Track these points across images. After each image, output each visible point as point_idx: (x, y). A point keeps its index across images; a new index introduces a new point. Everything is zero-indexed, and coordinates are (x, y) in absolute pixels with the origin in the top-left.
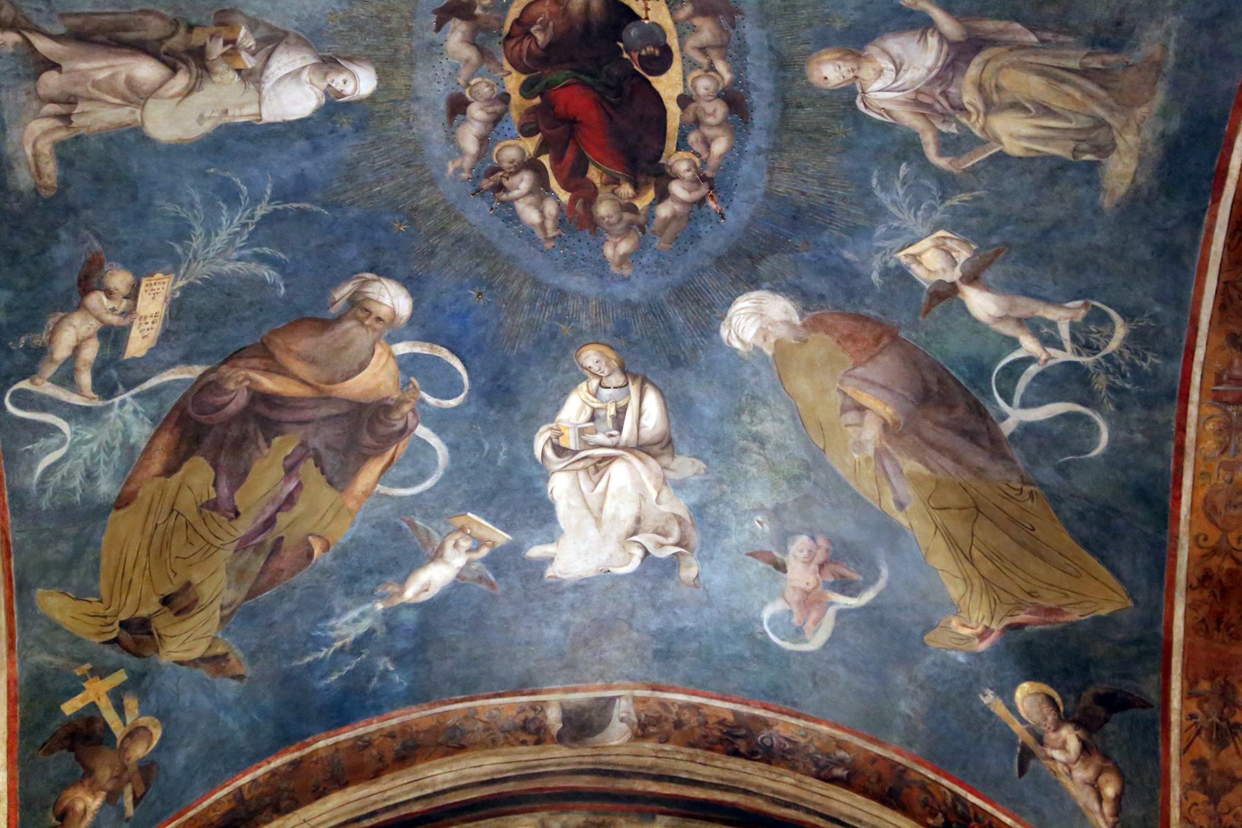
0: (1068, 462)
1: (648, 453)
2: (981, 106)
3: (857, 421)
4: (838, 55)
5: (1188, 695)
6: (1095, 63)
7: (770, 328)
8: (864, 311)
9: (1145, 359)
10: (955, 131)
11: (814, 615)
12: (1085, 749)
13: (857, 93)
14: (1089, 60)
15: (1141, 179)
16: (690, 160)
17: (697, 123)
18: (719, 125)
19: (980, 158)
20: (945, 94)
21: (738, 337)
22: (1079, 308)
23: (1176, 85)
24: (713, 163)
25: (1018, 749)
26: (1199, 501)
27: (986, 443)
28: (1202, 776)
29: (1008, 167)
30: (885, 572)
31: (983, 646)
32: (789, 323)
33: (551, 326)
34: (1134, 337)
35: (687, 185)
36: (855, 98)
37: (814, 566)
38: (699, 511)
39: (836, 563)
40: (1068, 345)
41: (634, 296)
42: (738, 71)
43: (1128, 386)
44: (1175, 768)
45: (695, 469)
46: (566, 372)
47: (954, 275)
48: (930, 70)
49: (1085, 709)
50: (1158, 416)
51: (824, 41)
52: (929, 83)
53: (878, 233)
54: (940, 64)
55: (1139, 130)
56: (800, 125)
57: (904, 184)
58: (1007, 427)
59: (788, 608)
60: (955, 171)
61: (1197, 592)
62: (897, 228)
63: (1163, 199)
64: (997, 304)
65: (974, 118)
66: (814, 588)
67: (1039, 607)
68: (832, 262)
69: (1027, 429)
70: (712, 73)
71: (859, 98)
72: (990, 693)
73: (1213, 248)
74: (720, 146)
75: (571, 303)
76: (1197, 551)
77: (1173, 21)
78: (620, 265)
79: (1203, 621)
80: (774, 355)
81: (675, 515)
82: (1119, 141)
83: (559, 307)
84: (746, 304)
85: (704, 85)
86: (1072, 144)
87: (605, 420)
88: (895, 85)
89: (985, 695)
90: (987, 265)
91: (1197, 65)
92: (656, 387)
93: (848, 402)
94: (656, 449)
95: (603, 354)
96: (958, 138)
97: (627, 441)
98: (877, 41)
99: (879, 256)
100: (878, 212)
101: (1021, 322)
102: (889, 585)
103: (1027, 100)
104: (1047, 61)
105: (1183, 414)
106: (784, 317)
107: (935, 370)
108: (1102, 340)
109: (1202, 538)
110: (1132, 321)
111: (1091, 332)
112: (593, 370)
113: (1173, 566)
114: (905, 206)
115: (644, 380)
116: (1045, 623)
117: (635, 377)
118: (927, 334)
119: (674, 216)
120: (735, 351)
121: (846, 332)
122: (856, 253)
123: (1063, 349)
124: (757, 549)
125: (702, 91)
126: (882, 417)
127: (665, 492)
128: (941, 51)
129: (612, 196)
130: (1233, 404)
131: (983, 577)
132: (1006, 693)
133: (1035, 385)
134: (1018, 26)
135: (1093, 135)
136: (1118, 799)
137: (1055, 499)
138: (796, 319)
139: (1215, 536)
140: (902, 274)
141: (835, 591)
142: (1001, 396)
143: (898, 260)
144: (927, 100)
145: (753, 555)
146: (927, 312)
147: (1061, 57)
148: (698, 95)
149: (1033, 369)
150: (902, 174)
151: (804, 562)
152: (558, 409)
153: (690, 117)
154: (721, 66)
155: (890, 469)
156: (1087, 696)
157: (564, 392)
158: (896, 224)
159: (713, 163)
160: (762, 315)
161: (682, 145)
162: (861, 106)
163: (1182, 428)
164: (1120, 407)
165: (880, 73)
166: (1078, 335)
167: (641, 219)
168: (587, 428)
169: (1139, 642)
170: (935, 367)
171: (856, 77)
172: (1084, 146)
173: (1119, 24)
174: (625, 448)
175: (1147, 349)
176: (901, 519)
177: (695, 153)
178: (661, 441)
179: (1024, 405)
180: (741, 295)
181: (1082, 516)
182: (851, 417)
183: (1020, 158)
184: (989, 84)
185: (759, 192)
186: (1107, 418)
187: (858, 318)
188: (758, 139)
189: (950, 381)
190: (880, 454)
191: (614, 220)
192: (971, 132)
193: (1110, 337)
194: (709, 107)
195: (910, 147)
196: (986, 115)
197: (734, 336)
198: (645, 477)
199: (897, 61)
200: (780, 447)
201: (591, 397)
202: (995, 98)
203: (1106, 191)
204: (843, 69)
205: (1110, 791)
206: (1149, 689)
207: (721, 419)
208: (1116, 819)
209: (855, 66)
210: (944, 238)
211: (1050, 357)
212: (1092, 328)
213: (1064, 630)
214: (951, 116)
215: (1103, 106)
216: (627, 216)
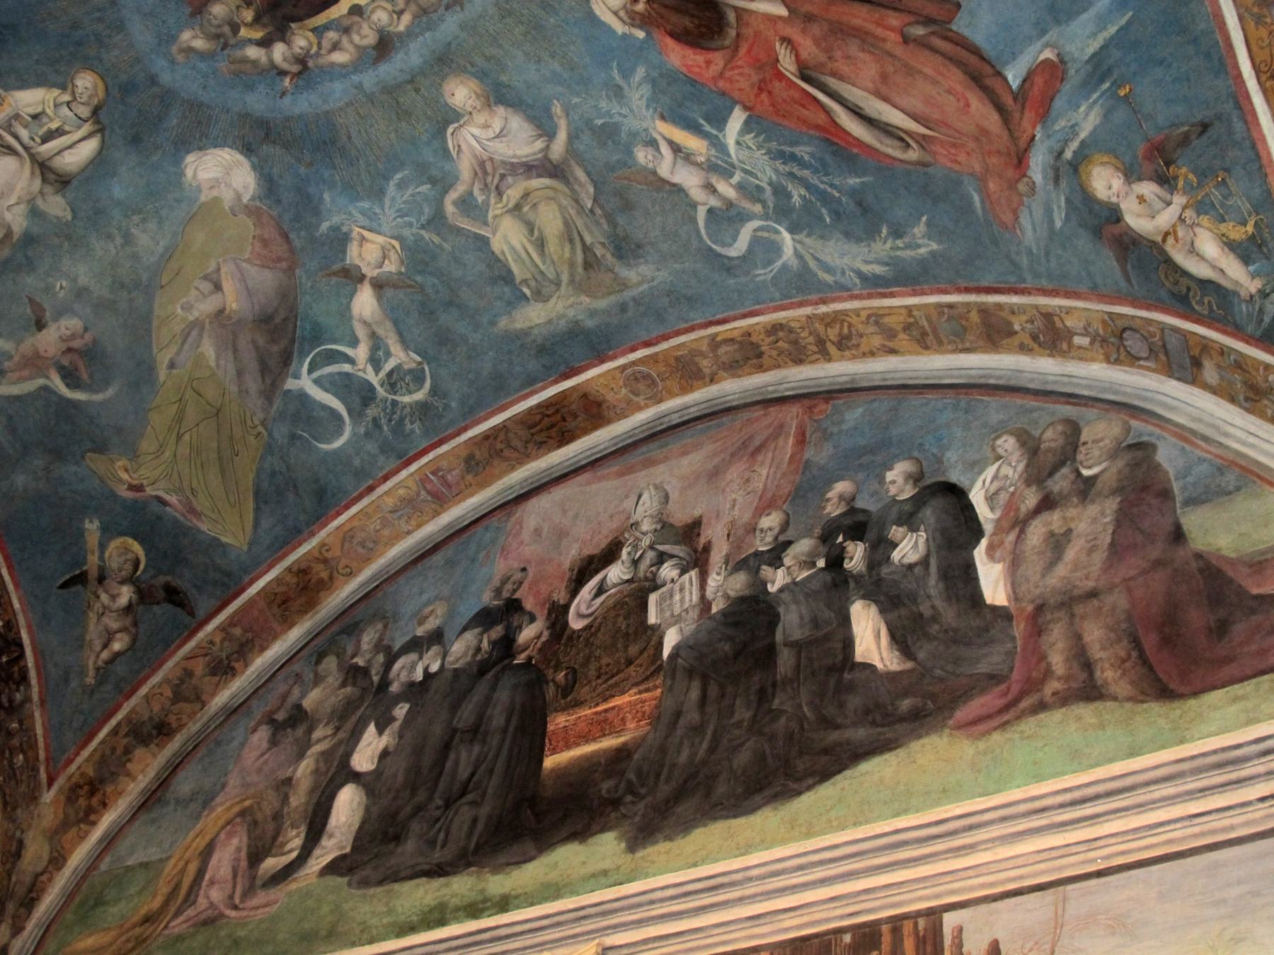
0: (301, 436)
1: (42, 173)
2: (511, 205)
3: (206, 292)
4: (479, 92)
5: (222, 628)
6: (599, 252)
7: (223, 185)
8: (292, 236)
9: (412, 423)
10: (480, 200)
11: (26, 373)
12: (129, 609)
13: (458, 121)
14: (598, 246)
15: (536, 331)
16: (311, 44)
17: (346, 31)
18: (357, 47)
19: (473, 229)
20: (503, 176)
21: (196, 169)
22: (414, 361)
23: (623, 308)
24: (321, 61)
25: (77, 572)
26: (346, 528)
27: (268, 381)
28: (182, 681)
29: (480, 250)
30: (110, 392)
31: (124, 493)
32: (239, 197)
33: (87, 35)
34: (423, 407)
35: (288, 54)
36: (453, 123)
37: (64, 347)
38: (29, 240)
39: (82, 357)
40: (382, 374)
41: (166, 78)
42: (410, 34)
43: (385, 428)
44: (170, 664)
45: (61, 214)
46: (57, 71)
47: (370, 272)
48: (515, 156)
49: (152, 586)
50: (382, 459)
51: (481, 76)
52: (503, 162)
53: (360, 204)
54: (524, 160)
55: (571, 306)
56: (401, 100)
57: (413, 195)
58: (291, 384)
59: (13, 353)
60: (450, 220)
61: (290, 575)
62: (375, 213)
63: (532, 352)
64: (373, 313)
65: (499, 206)
66: (47, 358)
67: (191, 502)
68: (312, 190)
69: (303, 396)
70: (395, 16)
71: (456, 125)
72: (97, 523)
73: (523, 403)
74: (339, 57)
75: (119, 37)
76: (316, 554)
77: (663, 275)
78: (182, 50)
79: (276, 594)
80: (203, 204)
81: (9, 227)
82: (553, 301)
83: (108, 31)
84: (228, 157)
85: (381, 17)
86: (529, 276)
87: (41, 126)
88: (485, 142)
89: (91, 522)
90: (395, 286)
91: (642, 309)
92: (103, 141)
93: (215, 276)
94: (52, 177)
95: (95, 87)
96: (476, 206)
97: (39, 153)
98: (510, 110)
99: (344, 217)
100: (379, 194)
101: (373, 335)
102: (102, 404)
103: (539, 229)
104: (579, 223)
105: (397, 471)
106: (241, 190)
107: (291, 311)
108: (404, 390)
109: (327, 548)
110: (433, 396)
111: (404, 380)
112: (76, 90)
113: (295, 548)
114: (397, 207)
115: (101, 130)
116: (183, 515)
117: (98, 122)
118: (312, 287)
119: (255, 63)
120: (182, 174)
121: (266, 236)
122: (333, 201)
123: (377, 375)
124: (38, 300)
125: (375, 17)
126: (225, 305)
127: (22, 206)
128: (535, 154)
129: (234, 8)
130: (428, 492)
131: (175, 455)
132: (109, 531)
133: (337, 377)
134: (592, 190)
135: (544, 283)
136: (118, 655)
137: (269, 448)
138: (245, 200)
139: (336, 552)
140: (340, 240)
141: (59, 373)
142: (310, 363)
143: (351, 231)
144: (489, 167)
145: (31, 300)
146: (329, 275)
147: (588, 228)
148: (369, 17)
149: (347, 368)
150: (419, 189)
151: (60, 337)
152: (24, 85)
153: (346, 22)
154: (406, 18)
155: (190, 340)
156: (162, 579)
157: (41, 82)
158: (378, 210)
159: (321, 61)
160: (228, 173)
161: (319, 31)
162: (450, 130)
163: (386, 478)
164: (367, 434)
165: (486, 126)
166: (395, 376)
167: (232, 41)
168: (23, 118)
169: (229, 575)
170: (293, 310)
171: (471, 113)
172: (533, 283)
173: (639, 246)
174: (33, 157)
175: (420, 419)
176: (162, 374)
177: (319, 44)
178: (61, 176)
179: (317, 382)
180: (232, 148)
181: (273, 474)
182: (207, 287)
183: (493, 253)
184: (533, 198)
185: (326, 108)
186: (354, 434)
187: (286, 236)
188: (369, 79)
189: (291, 326)
190: (197, 324)
191: (215, 22)
192: (487, 211)
193: (410, 393)
194: (366, 30)
195: (443, 183)
196: (507, 212)
197: (193, 167)
198: (19, 186)
199: (504, 132)
200: (135, 257)
201: (52, 104)
202: (526, 209)
203: (511, 317)
204: (470, 102)
205: (117, 646)
206: (202, 607)
207: (119, 203)
208: (104, 665)
209: (479, 107)
210: (394, 247)
211: (364, 371)
212: (408, 378)
213: (190, 528)
214: (489, 191)
215: (572, 275)
216: (226, 29)
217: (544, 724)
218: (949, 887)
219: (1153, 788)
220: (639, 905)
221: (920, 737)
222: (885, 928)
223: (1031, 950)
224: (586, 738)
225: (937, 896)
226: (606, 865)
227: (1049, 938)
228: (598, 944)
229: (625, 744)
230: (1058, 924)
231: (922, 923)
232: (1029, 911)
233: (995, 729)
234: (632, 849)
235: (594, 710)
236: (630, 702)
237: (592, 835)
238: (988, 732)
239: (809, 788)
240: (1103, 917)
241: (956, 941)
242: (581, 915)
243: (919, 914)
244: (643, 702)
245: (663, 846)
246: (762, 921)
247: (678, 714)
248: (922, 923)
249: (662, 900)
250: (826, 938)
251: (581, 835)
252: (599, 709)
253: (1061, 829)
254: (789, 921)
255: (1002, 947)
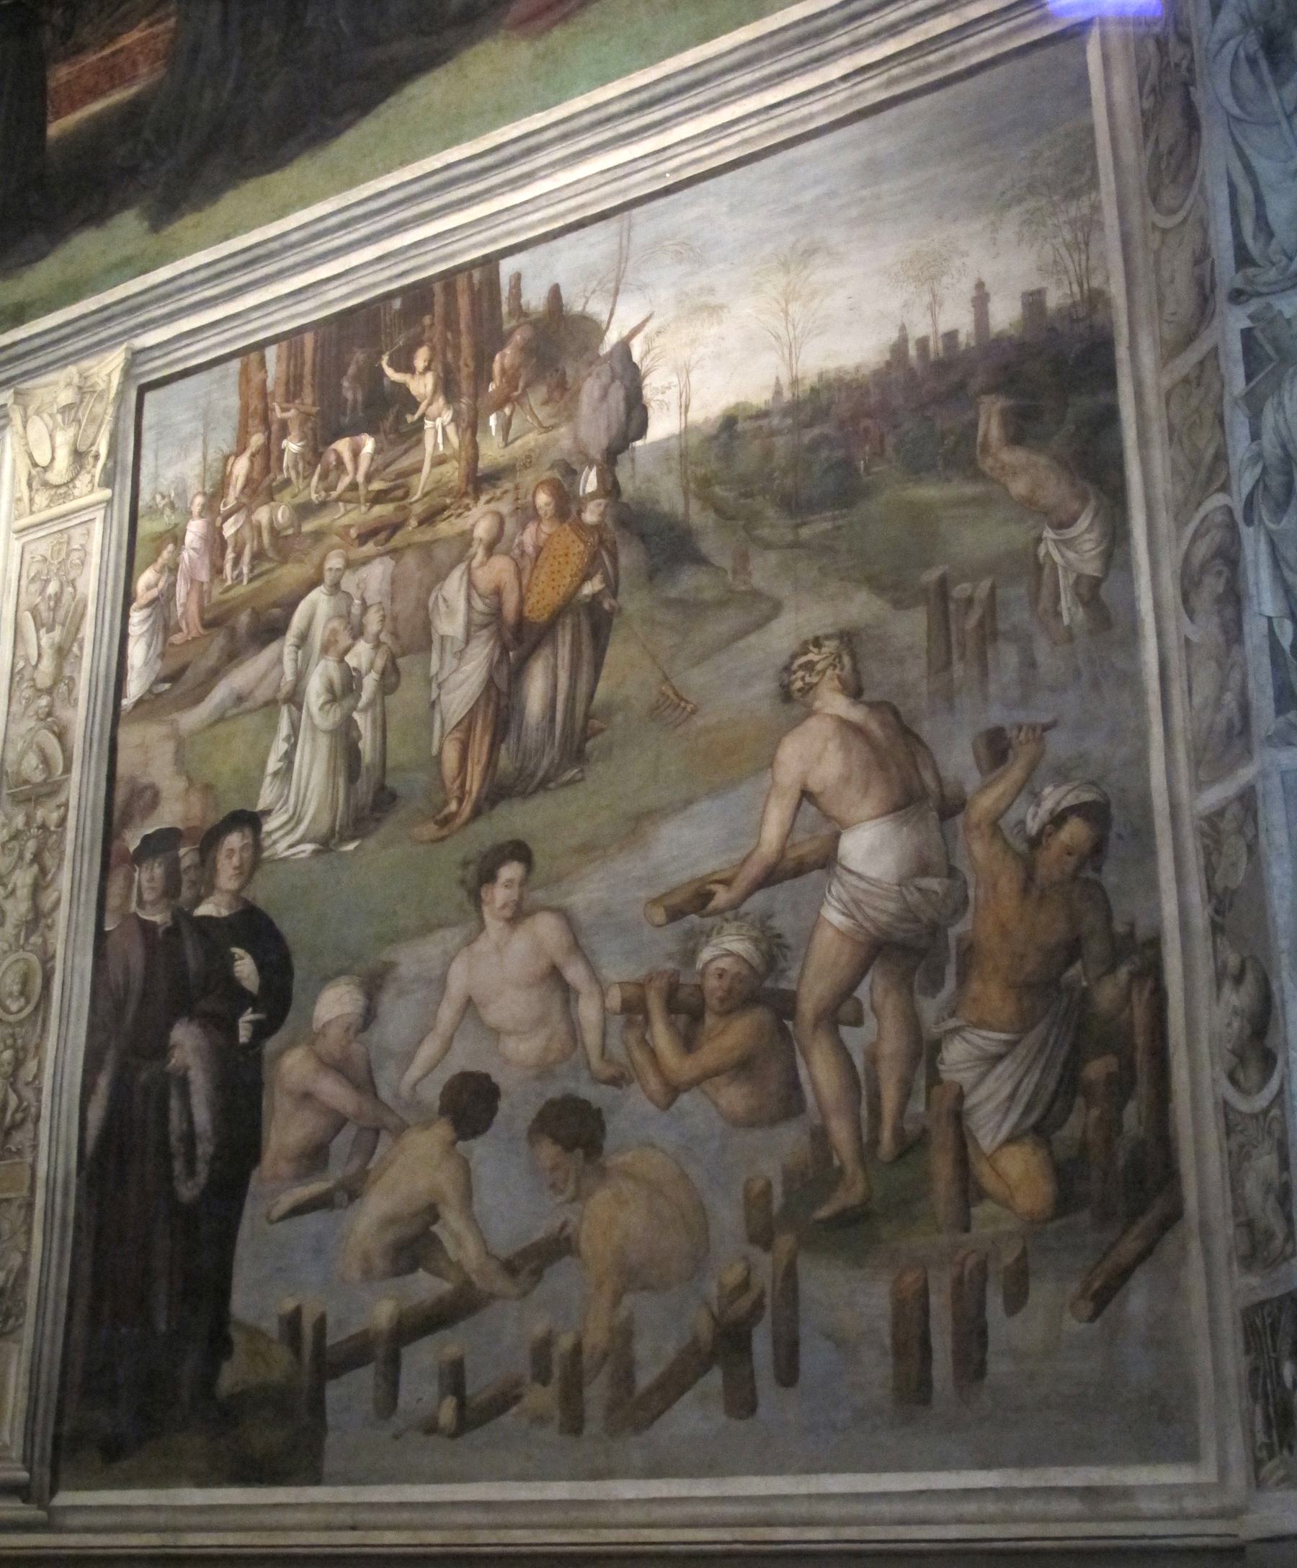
217: (43, 82)
218: (504, 228)
219: (728, 77)
220: (168, 296)
221: (472, 43)
222: (437, 288)
223: (593, 292)
224: (94, 93)
225: (493, 240)
226: (129, 250)
227: (612, 276)
228: (127, 349)
229: (138, 95)
230: (622, 256)
231: (477, 275)
232: (592, 245)
233: (555, 23)
234: (155, 228)
235: (99, 55)
236: (140, 39)
237: (111, 215)
238: (549, 28)
239: (349, 125)
240: (671, 242)
241: (514, 291)
242: (105, 316)
243: (473, 264)
244: (155, 36)
245: (190, 220)
246: (302, 297)
247: (195, 50)
248: (477, 275)
249: (193, 286)
250: (373, 307)
251: (98, 217)
252: (107, 52)
253: (627, 141)
254: (334, 292)
255: (564, 293)
